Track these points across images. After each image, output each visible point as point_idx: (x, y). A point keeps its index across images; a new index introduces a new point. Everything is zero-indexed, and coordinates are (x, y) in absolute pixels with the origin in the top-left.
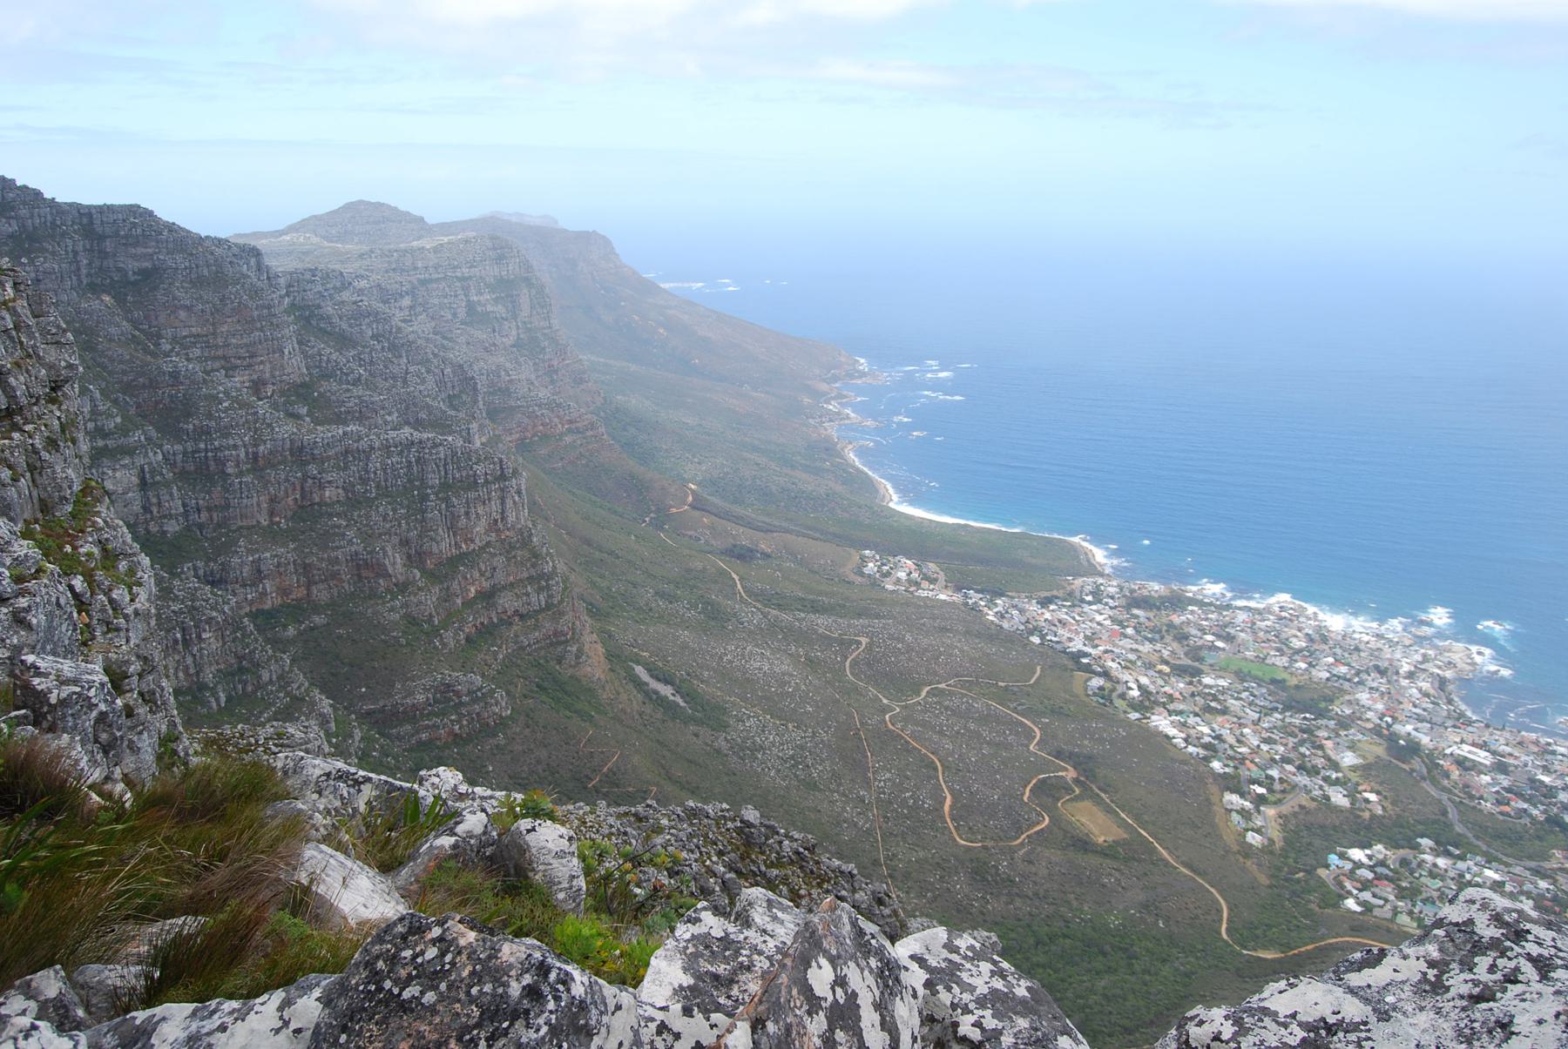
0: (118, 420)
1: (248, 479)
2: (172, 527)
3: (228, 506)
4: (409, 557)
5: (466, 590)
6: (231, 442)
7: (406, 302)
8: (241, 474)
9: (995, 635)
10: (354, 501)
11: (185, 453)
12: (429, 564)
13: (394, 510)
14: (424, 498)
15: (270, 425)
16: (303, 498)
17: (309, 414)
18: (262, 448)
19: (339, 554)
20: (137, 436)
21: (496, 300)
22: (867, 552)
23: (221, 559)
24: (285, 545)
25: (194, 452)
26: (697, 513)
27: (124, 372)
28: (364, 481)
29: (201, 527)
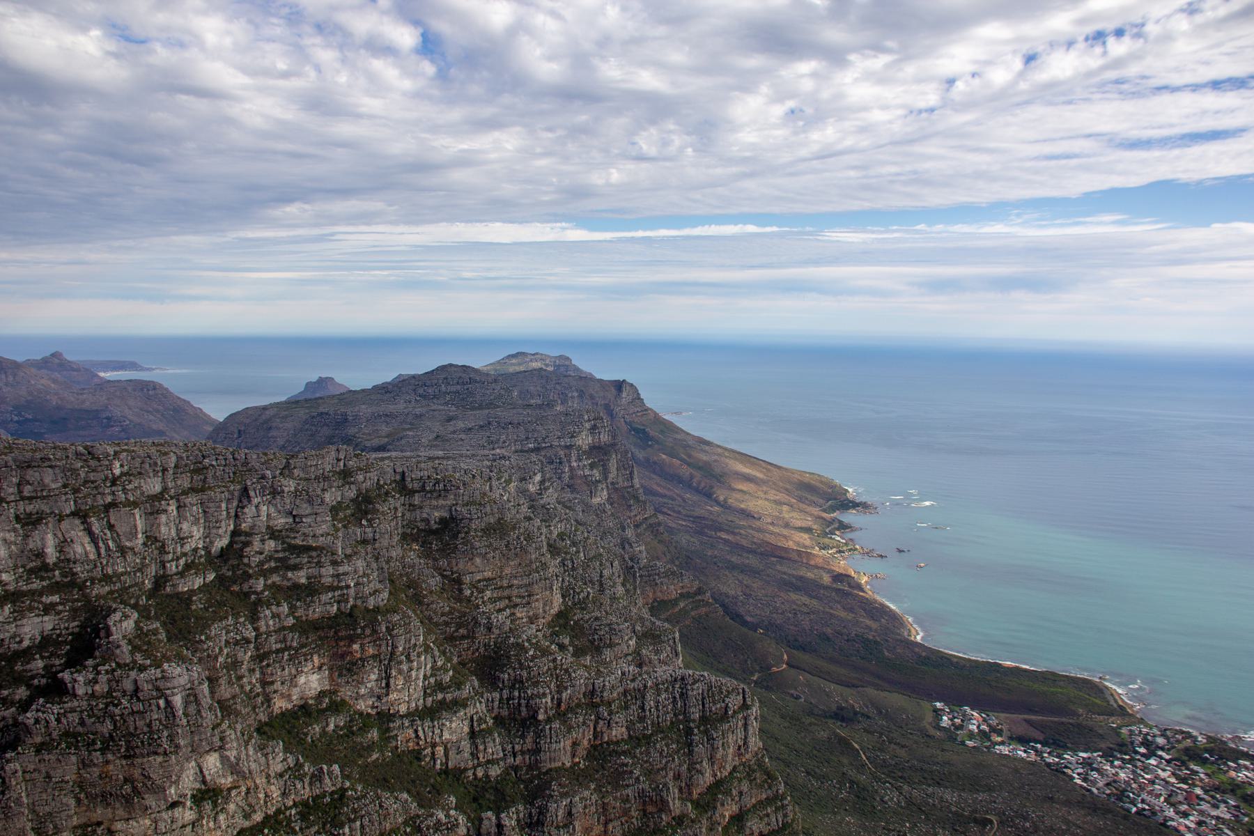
0: (451, 673)
1: (556, 725)
2: (495, 771)
3: (537, 751)
4: (681, 790)
5: (723, 816)
6: (541, 691)
7: (538, 478)
8: (549, 720)
9: (1091, 805)
10: (638, 740)
11: (501, 699)
12: (695, 796)
13: (667, 745)
14: (689, 732)
15: (566, 671)
16: (595, 737)
17: (571, 641)
18: (564, 695)
19: (629, 791)
20: (466, 691)
21: (592, 466)
22: (938, 705)
23: (538, 802)
24: (588, 788)
25: (508, 699)
26: (793, 671)
27: (447, 624)
28: (642, 719)
29: (516, 769)
